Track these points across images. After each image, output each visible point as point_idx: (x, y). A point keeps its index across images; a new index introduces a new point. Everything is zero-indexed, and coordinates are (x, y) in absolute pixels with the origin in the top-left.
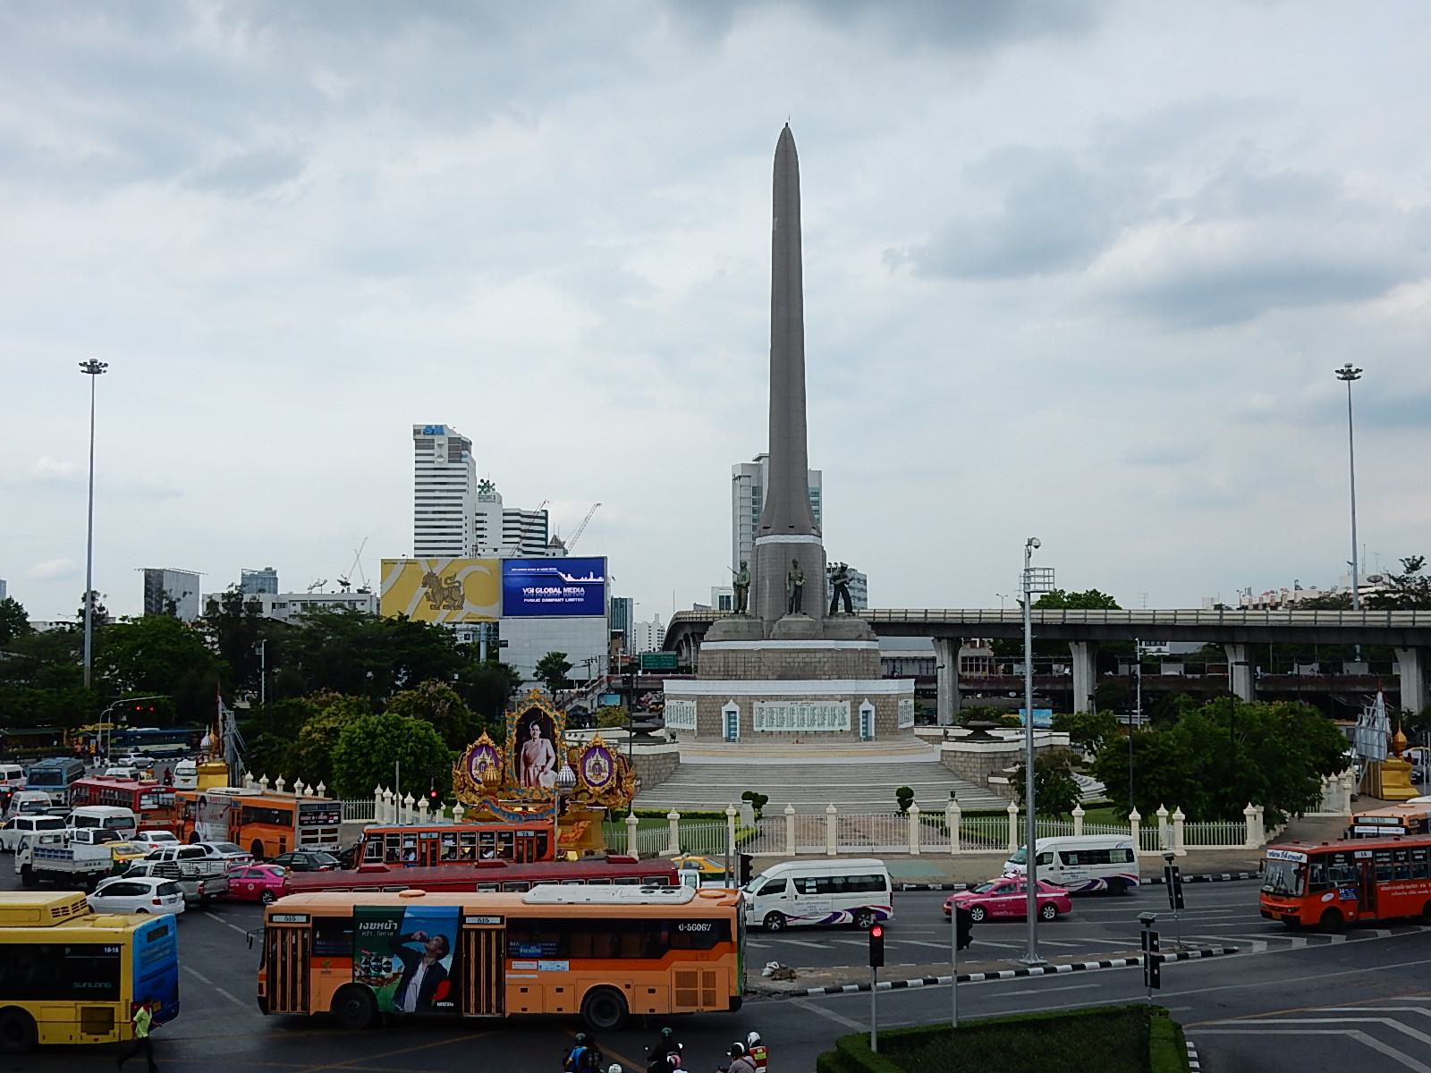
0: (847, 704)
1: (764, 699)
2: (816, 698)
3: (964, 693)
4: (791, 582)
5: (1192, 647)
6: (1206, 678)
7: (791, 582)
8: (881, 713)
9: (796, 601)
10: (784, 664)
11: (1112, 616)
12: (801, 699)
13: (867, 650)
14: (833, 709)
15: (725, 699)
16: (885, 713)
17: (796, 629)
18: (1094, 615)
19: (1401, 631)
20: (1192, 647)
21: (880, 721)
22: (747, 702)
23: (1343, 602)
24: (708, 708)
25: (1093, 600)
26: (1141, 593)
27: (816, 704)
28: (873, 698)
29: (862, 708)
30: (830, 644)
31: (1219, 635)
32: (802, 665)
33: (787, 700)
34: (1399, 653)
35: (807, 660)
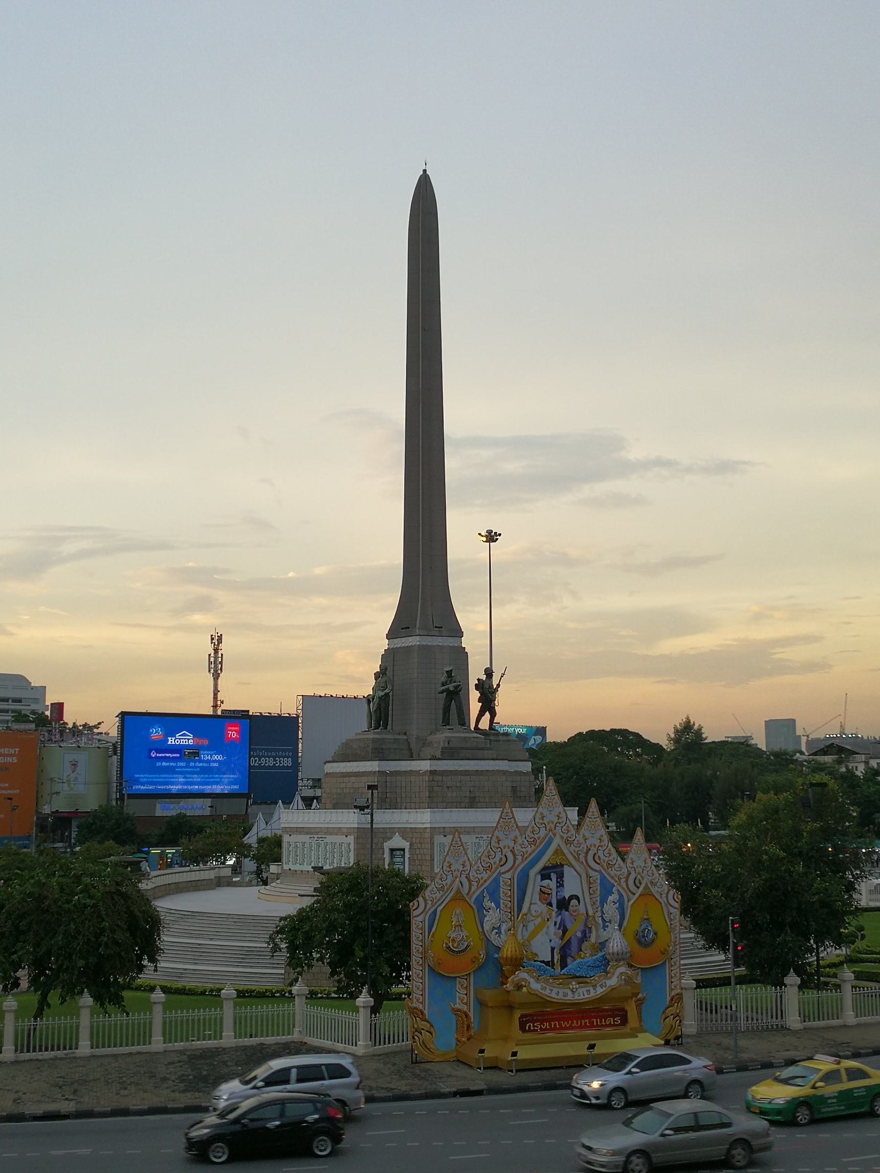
0: (351, 839)
2: (330, 831)
8: (418, 851)
10: (339, 791)
12: (317, 833)
13: (433, 773)
14: (341, 845)
16: (422, 851)
21: (417, 862)
27: (330, 839)
28: (405, 833)
29: (388, 845)
30: (373, 766)
32: (352, 791)
33: (307, 833)
35: (356, 785)
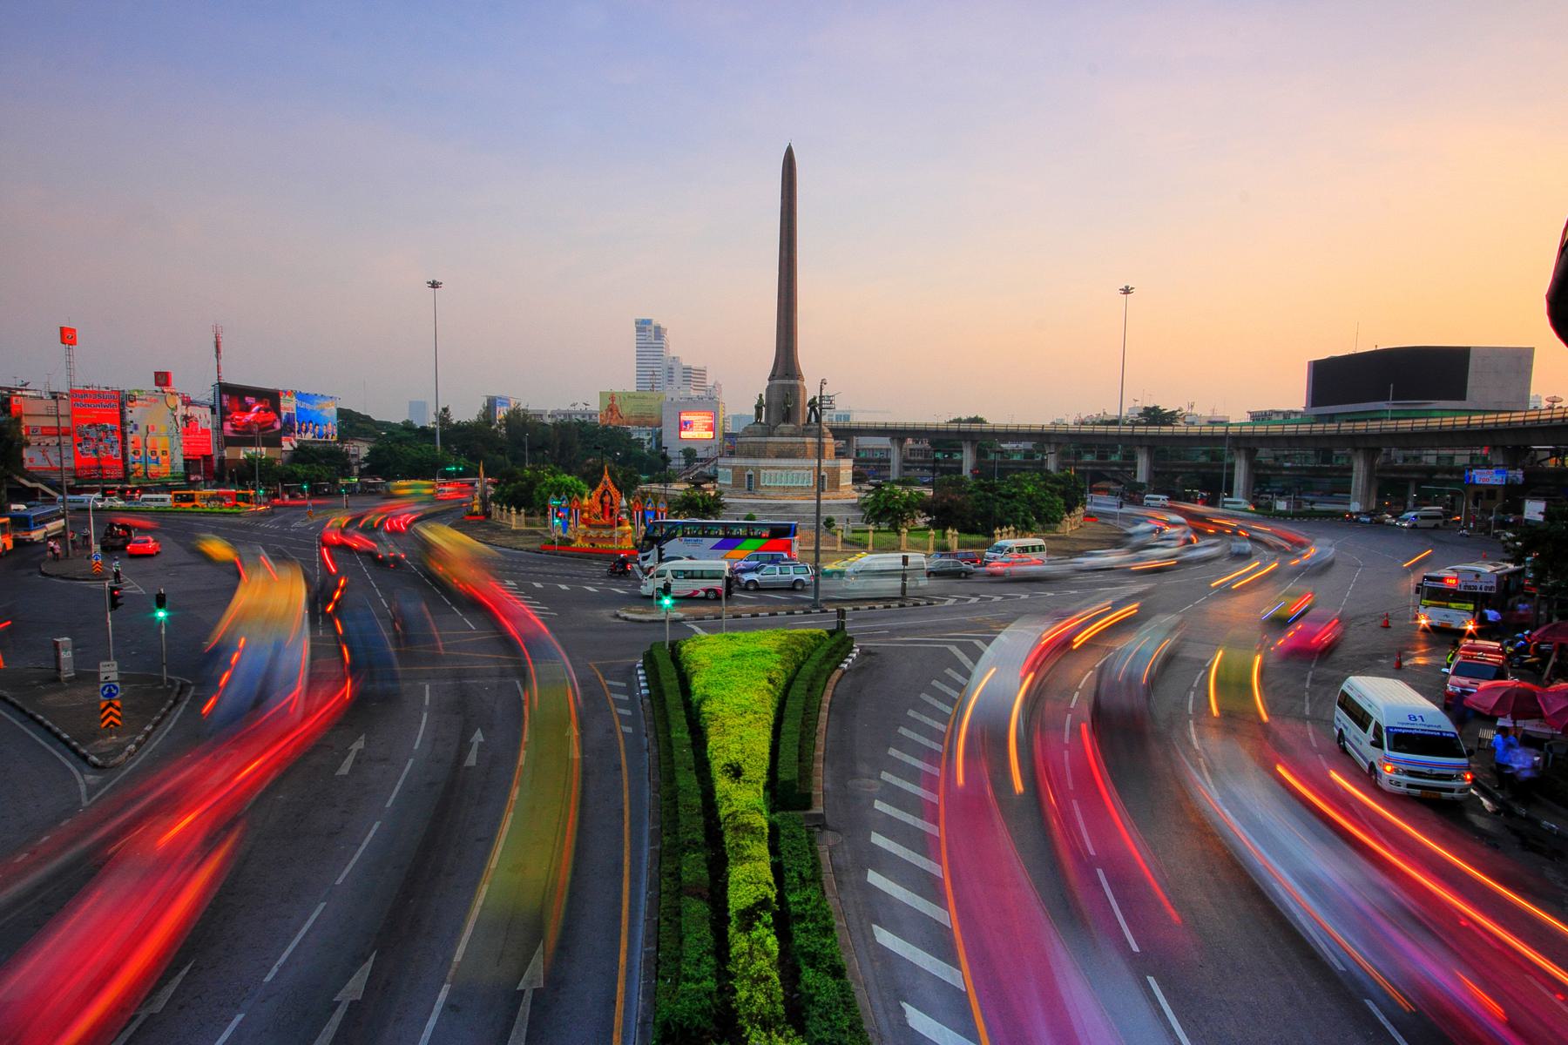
1: (766, 468)
3: (907, 469)
4: (786, 406)
5: (1028, 445)
6: (1031, 463)
7: (786, 406)
9: (788, 416)
11: (984, 427)
15: (747, 468)
17: (786, 431)
18: (975, 427)
19: (1140, 437)
20: (1028, 445)
22: (757, 470)
23: (1115, 422)
24: (738, 472)
25: (977, 420)
26: (997, 418)
31: (1043, 438)
34: (1138, 450)
